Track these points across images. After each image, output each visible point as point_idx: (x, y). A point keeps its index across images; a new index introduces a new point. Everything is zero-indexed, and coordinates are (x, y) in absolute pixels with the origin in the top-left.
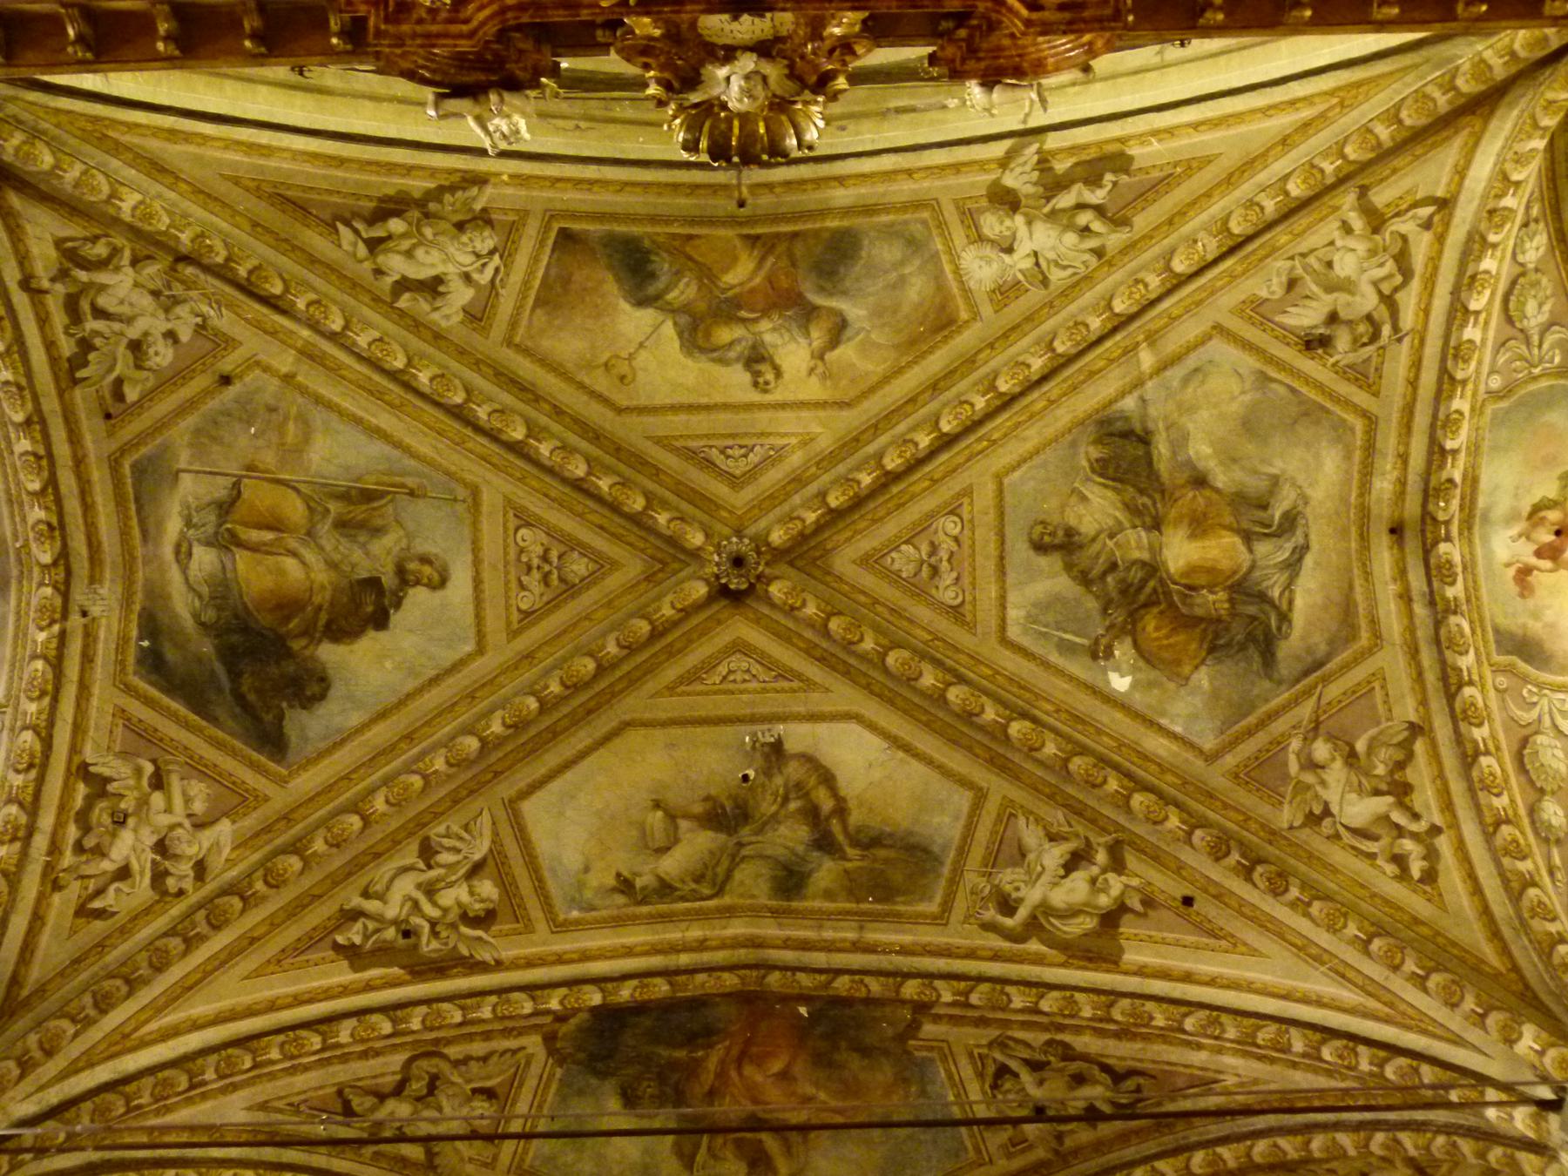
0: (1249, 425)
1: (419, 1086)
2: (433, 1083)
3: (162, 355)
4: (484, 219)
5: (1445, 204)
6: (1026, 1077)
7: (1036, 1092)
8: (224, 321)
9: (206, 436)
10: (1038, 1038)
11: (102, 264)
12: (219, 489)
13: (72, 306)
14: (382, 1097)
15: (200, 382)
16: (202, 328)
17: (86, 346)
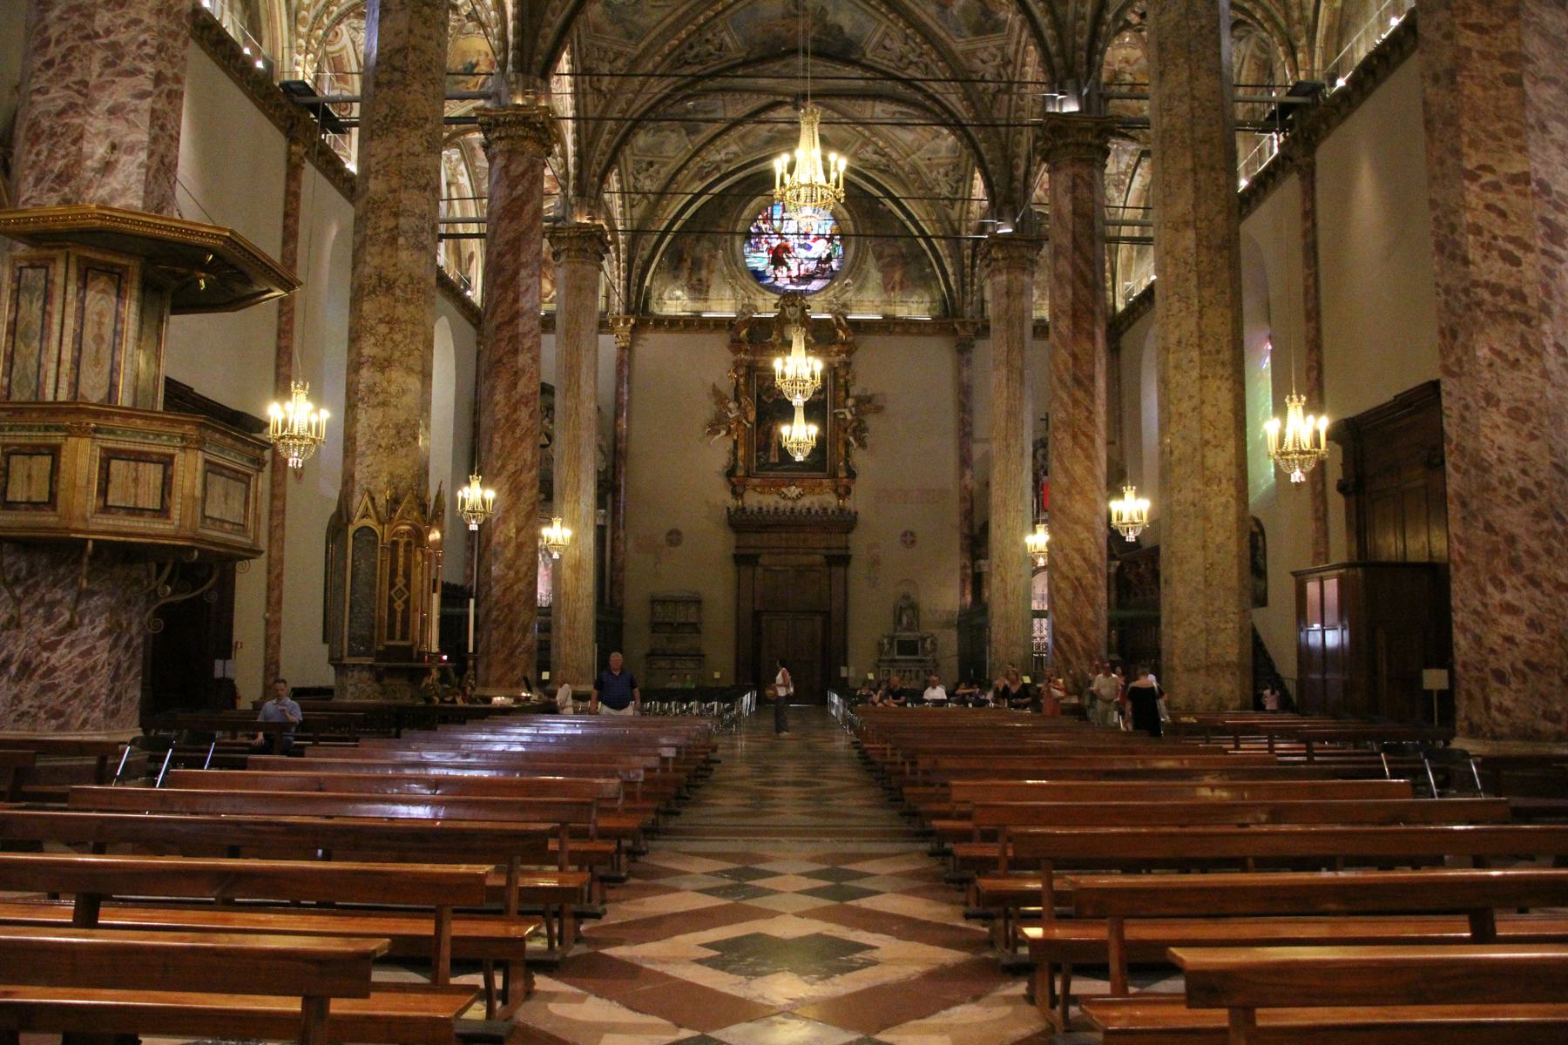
0: (663, 143)
1: (905, 61)
2: (901, 59)
3: (942, 170)
4: (860, 160)
5: (632, 206)
6: (713, 50)
7: (710, 47)
8: (925, 170)
9: (936, 152)
10: (712, 63)
11: (947, 198)
12: (938, 141)
13: (956, 192)
14: (916, 63)
15: (936, 161)
16: (931, 172)
17: (957, 182)
